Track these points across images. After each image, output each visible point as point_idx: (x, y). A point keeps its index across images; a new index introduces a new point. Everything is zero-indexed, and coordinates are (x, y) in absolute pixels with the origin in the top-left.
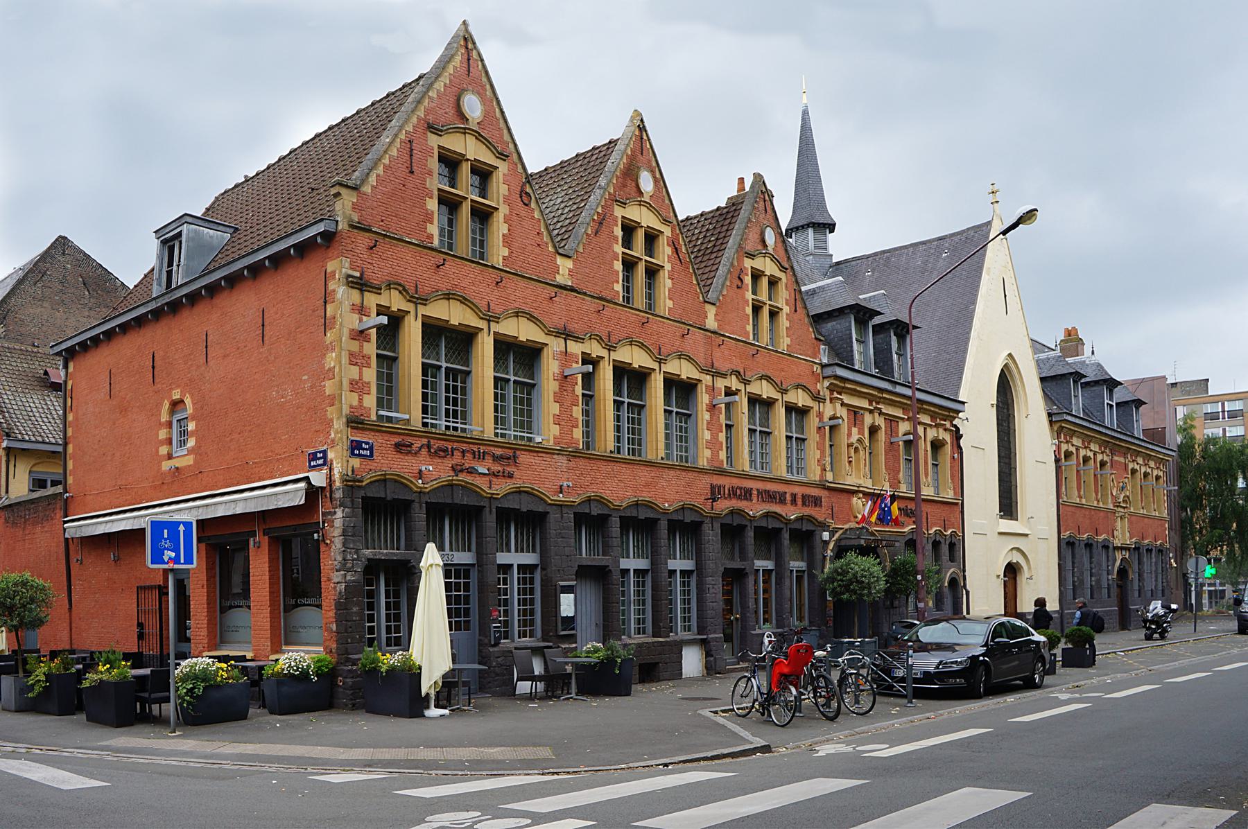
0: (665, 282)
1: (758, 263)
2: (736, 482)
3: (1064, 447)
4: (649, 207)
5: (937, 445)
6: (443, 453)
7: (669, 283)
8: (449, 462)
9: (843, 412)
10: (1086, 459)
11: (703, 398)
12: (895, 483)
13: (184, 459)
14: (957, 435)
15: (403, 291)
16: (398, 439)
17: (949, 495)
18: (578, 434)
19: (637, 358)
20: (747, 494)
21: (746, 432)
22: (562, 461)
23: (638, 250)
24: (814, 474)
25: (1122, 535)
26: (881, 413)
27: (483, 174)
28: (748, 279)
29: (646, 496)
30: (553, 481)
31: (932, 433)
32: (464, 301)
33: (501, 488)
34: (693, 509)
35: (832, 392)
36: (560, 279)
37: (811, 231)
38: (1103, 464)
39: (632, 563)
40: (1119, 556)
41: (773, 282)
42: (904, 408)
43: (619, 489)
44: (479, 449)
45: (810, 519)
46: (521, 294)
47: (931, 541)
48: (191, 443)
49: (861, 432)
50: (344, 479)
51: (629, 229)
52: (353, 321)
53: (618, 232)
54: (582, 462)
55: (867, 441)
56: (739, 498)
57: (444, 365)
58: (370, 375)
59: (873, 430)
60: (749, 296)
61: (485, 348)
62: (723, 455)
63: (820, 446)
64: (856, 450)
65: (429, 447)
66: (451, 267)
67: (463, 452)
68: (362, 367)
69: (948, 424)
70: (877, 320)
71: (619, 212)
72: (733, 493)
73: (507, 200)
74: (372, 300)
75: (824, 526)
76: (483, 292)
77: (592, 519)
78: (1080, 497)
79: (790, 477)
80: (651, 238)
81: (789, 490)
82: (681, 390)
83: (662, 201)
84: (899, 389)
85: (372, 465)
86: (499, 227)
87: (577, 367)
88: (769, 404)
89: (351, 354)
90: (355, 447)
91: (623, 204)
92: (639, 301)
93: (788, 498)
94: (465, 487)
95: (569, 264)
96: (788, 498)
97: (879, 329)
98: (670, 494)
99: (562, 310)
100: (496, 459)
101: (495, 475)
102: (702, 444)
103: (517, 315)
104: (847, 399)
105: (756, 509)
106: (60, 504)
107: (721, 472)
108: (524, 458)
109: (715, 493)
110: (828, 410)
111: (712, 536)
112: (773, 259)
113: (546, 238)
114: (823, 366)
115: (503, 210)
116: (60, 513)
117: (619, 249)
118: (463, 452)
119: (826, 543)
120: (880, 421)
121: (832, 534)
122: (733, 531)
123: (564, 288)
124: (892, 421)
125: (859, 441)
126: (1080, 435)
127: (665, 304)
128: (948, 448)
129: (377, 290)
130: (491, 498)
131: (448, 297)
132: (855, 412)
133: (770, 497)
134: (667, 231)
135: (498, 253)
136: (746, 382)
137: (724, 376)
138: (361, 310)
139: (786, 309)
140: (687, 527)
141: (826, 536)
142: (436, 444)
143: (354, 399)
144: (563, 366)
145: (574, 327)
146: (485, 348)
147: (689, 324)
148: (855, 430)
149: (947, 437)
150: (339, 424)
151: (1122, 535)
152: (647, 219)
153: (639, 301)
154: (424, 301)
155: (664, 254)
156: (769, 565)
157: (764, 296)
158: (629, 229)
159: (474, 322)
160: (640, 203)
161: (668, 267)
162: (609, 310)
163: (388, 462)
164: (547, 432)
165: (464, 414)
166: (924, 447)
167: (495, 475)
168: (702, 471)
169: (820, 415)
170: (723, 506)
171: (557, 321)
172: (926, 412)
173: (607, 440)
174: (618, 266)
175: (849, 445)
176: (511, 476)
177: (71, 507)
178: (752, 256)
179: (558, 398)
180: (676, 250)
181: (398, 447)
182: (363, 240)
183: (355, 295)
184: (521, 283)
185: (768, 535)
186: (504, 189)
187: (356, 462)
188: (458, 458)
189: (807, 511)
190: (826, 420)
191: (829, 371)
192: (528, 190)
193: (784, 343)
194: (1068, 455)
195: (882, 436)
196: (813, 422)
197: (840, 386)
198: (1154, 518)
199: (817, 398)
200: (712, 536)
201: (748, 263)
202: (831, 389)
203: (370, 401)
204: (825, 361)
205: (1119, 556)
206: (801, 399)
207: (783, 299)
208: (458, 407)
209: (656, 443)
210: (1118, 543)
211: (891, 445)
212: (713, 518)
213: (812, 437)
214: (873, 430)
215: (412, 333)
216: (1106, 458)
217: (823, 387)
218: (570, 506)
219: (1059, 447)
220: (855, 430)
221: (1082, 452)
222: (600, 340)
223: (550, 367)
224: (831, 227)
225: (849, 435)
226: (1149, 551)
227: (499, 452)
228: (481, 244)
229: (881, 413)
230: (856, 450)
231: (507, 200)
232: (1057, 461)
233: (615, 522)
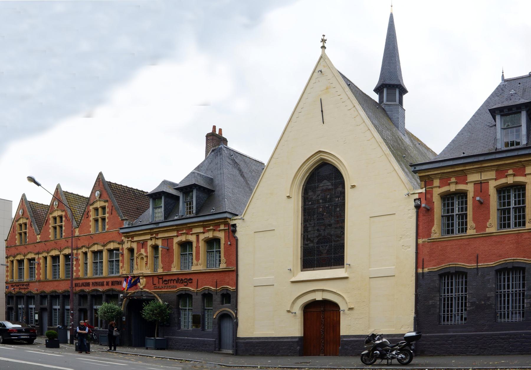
1: (95, 206)
20: (88, 284)
22: (37, 283)
30: (34, 289)
43: (48, 289)
45: (113, 290)
47: (219, 294)
51: (55, 218)
54: (41, 283)
69: (222, 227)
72: (83, 285)
77: (43, 296)
84: (160, 225)
93: (105, 283)
94: (20, 292)
95: (39, 236)
96: (105, 283)
99: (38, 248)
108: (31, 284)
123: (39, 242)
124: (169, 239)
140: (66, 297)
145: (41, 251)
170: (78, 289)
173: (49, 276)
185: (97, 297)
209: (62, 274)
212: (76, 293)
214: (155, 248)
222: (45, 251)
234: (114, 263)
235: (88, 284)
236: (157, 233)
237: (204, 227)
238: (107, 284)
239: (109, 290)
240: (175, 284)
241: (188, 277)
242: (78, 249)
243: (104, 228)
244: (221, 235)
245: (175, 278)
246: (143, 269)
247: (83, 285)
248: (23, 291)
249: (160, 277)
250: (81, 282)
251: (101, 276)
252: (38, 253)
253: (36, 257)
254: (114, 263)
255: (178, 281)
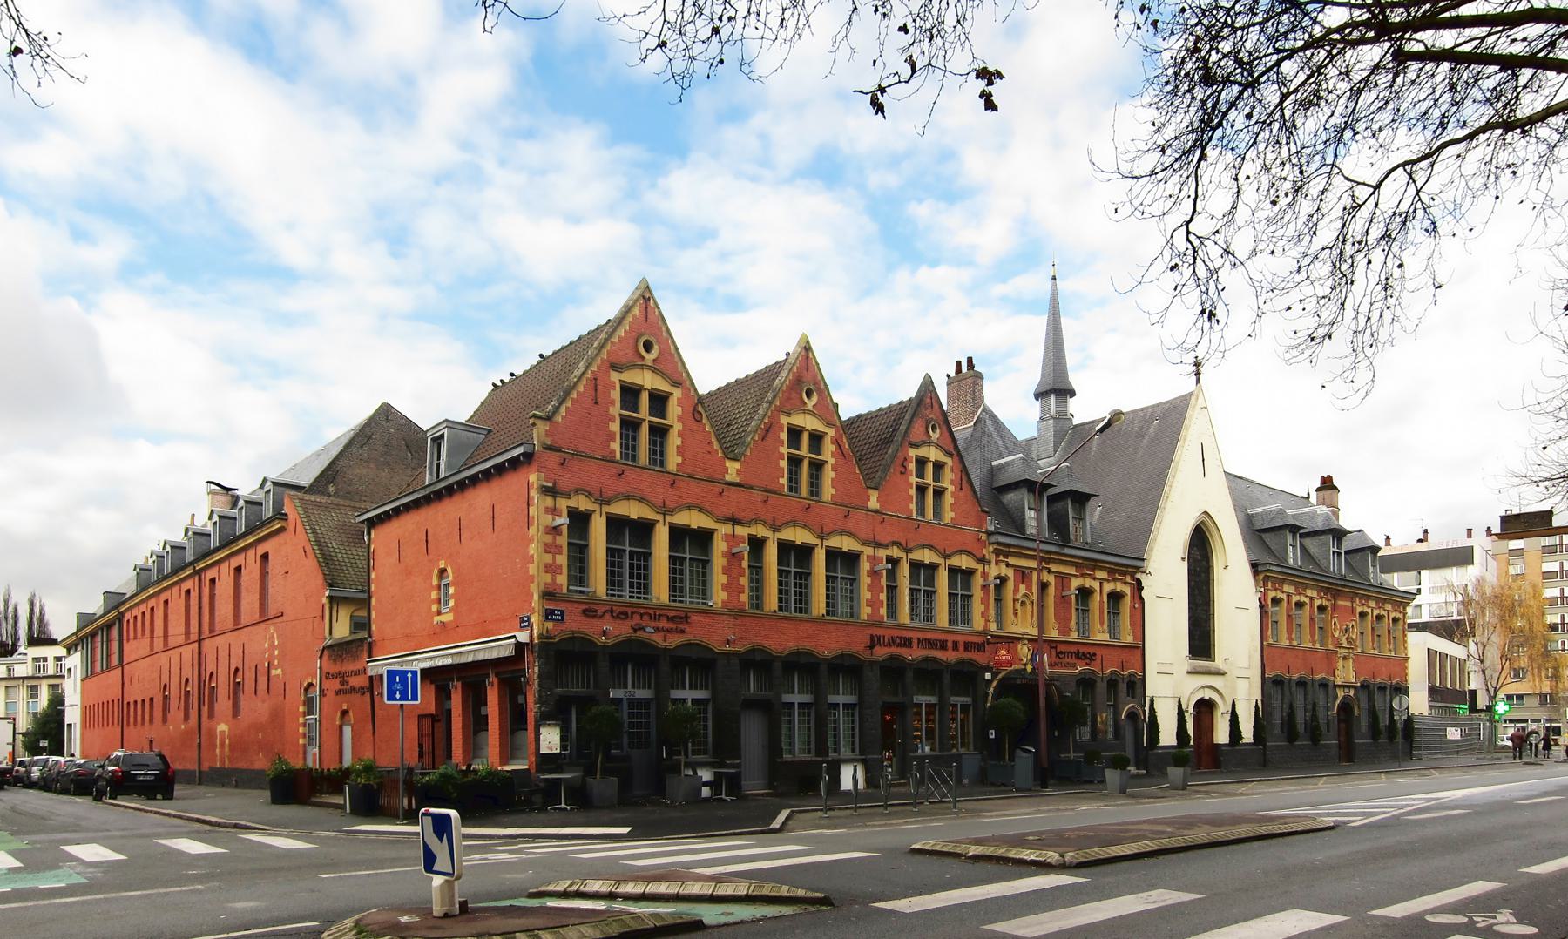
0: (828, 475)
2: (896, 633)
3: (1271, 594)
4: (812, 414)
5: (1115, 597)
6: (623, 616)
7: (832, 474)
8: (629, 623)
9: (1010, 573)
10: (1300, 605)
11: (865, 566)
12: (1064, 629)
13: (447, 617)
14: (1138, 587)
15: (589, 494)
16: (585, 607)
17: (1128, 639)
18: (744, 598)
19: (800, 536)
20: (907, 643)
21: (907, 592)
23: (805, 449)
24: (978, 623)
25: (1345, 673)
26: (1050, 571)
27: (659, 402)
28: (912, 466)
29: (807, 645)
30: (721, 637)
31: (1108, 587)
32: (641, 500)
33: (674, 641)
34: (852, 656)
35: (997, 555)
36: (728, 478)
37: (1053, 397)
38: (1322, 609)
39: (797, 698)
40: (1341, 693)
41: (939, 466)
42: (1077, 565)
43: (781, 641)
44: (656, 613)
45: (971, 663)
46: (694, 491)
48: (452, 603)
49: (1029, 588)
50: (541, 636)
52: (549, 520)
53: (784, 436)
55: (1035, 598)
56: (899, 645)
57: (628, 549)
58: (562, 560)
59: (1043, 586)
60: (913, 480)
61: (662, 537)
62: (883, 611)
63: (985, 601)
64: (1023, 603)
65: (612, 611)
66: (630, 474)
67: (641, 615)
68: (554, 554)
69: (1128, 579)
70: (1052, 491)
71: (784, 420)
72: (893, 642)
73: (680, 419)
74: (563, 504)
75: (988, 669)
76: (660, 492)
77: (757, 662)
78: (1291, 640)
79: (954, 627)
80: (817, 439)
81: (950, 638)
82: (843, 562)
83: (828, 409)
85: (564, 627)
86: (674, 441)
87: (745, 546)
88: (933, 567)
89: (546, 545)
90: (548, 614)
91: (788, 414)
92: (805, 489)
93: (950, 645)
95: (737, 465)
96: (950, 645)
97: (1053, 499)
98: (828, 645)
99: (733, 502)
100: (670, 619)
101: (669, 631)
102: (863, 603)
103: (689, 508)
104: (1012, 561)
105: (914, 654)
106: (366, 647)
107: (881, 624)
108: (694, 618)
109: (874, 641)
110: (994, 571)
111: (872, 679)
112: (938, 446)
113: (716, 446)
114: (989, 534)
115: (678, 427)
116: (365, 654)
117: (784, 450)
118: (641, 615)
119: (989, 682)
120: (1051, 579)
121: (995, 675)
122: (893, 670)
124: (1063, 579)
125: (1025, 595)
126: (1291, 583)
127: (828, 491)
128: (1128, 600)
129: (567, 496)
130: (666, 649)
131: (628, 497)
132: (1023, 574)
133: (931, 644)
134: (831, 432)
135: (673, 461)
136: (908, 550)
137: (885, 546)
138: (554, 511)
139: (951, 488)
141: (988, 676)
142: (617, 610)
143: (548, 578)
144: (730, 547)
145: (738, 515)
146: (662, 537)
147: (849, 506)
148: (1022, 588)
149: (1127, 590)
150: (536, 597)
151: (1345, 673)
152: (810, 423)
153: (805, 489)
154: (608, 502)
155: (828, 451)
156: (933, 700)
157: (929, 479)
158: (795, 434)
159: (649, 514)
160: (804, 412)
161: (831, 461)
162: (773, 499)
163: (576, 624)
164: (718, 597)
165: (646, 586)
166: (1098, 602)
167: (669, 631)
168: (862, 625)
169: (985, 575)
170: (881, 652)
171: (728, 513)
172: (1102, 569)
173: (772, 601)
174: (784, 464)
175: (1015, 600)
176: (683, 632)
177: (375, 650)
178: (916, 446)
179: (726, 571)
180: (840, 447)
181: (585, 612)
182: (553, 459)
183: (549, 501)
184: (693, 483)
186: (679, 410)
187: (550, 625)
188: (636, 619)
189: (967, 655)
190: (991, 578)
191: (993, 539)
192: (700, 408)
193: (948, 516)
194: (1276, 601)
195: (1052, 590)
196: (978, 581)
197: (1003, 552)
198: (1389, 658)
199: (982, 560)
200: (872, 679)
201: (913, 453)
202: (997, 553)
203: (562, 579)
204: (992, 529)
205: (1341, 693)
206: (964, 562)
207: (948, 481)
208: (642, 580)
209: (818, 604)
210: (1338, 682)
211: (1062, 600)
212: (872, 663)
213: (977, 593)
214: (1043, 586)
215: (598, 528)
216: (1325, 603)
217: (988, 552)
218: (736, 655)
219: (1265, 594)
220: (1022, 588)
221: (1295, 599)
223: (719, 546)
224: (1072, 393)
225: (1016, 590)
226: (1382, 689)
227: (672, 614)
228: (658, 455)
229: (1050, 571)
230: (1023, 603)
231: (680, 419)
232: (1261, 607)
233: (778, 666)
234: (960, 603)
235: (907, 643)
236: (1049, 561)
237: (1111, 572)
238: (955, 646)
239: (962, 662)
240: (1074, 661)
241: (1092, 650)
242: (877, 545)
243: (938, 513)
244: (1127, 590)
245: (1073, 649)
246: (1022, 625)
247: (893, 642)
248: (657, 639)
249: (1052, 644)
250: (888, 633)
251: (965, 628)
252: (734, 521)
253: (724, 529)
254: (960, 603)
255: (1079, 656)
